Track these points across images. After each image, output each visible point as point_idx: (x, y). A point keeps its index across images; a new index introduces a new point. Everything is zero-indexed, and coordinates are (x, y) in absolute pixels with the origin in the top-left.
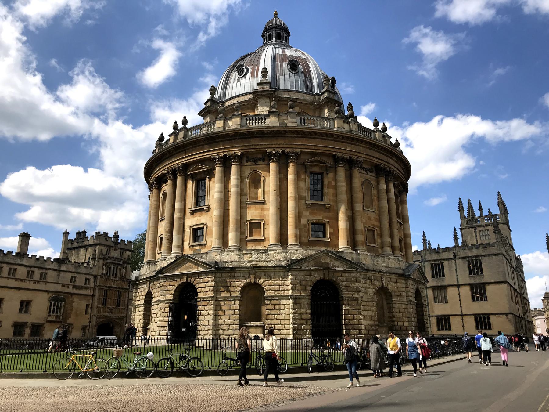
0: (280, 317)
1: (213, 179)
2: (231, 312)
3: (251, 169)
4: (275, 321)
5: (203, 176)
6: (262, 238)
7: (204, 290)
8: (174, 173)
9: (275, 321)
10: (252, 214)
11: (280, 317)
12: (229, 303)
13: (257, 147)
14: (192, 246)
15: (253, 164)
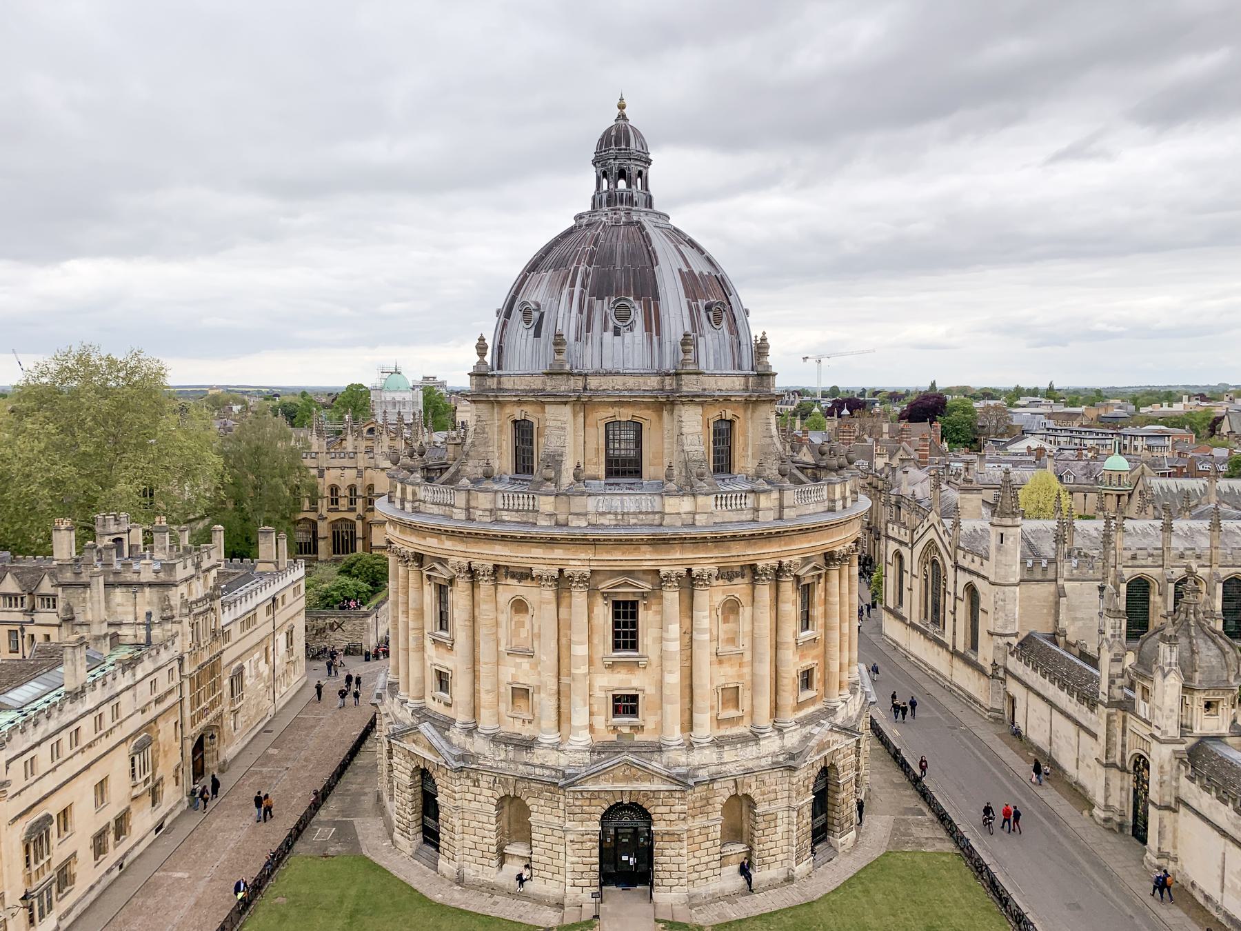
0: (775, 837)
1: (654, 608)
2: (709, 844)
3: (723, 593)
4: (770, 845)
5: (631, 598)
6: (740, 713)
7: (667, 817)
8: (562, 582)
9: (770, 845)
10: (728, 675)
11: (775, 837)
12: (706, 831)
13: (742, 558)
14: (615, 728)
15: (727, 583)
